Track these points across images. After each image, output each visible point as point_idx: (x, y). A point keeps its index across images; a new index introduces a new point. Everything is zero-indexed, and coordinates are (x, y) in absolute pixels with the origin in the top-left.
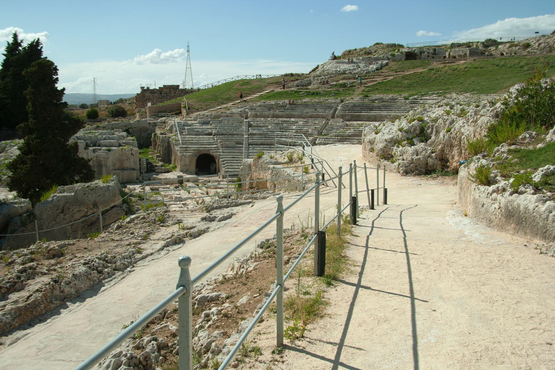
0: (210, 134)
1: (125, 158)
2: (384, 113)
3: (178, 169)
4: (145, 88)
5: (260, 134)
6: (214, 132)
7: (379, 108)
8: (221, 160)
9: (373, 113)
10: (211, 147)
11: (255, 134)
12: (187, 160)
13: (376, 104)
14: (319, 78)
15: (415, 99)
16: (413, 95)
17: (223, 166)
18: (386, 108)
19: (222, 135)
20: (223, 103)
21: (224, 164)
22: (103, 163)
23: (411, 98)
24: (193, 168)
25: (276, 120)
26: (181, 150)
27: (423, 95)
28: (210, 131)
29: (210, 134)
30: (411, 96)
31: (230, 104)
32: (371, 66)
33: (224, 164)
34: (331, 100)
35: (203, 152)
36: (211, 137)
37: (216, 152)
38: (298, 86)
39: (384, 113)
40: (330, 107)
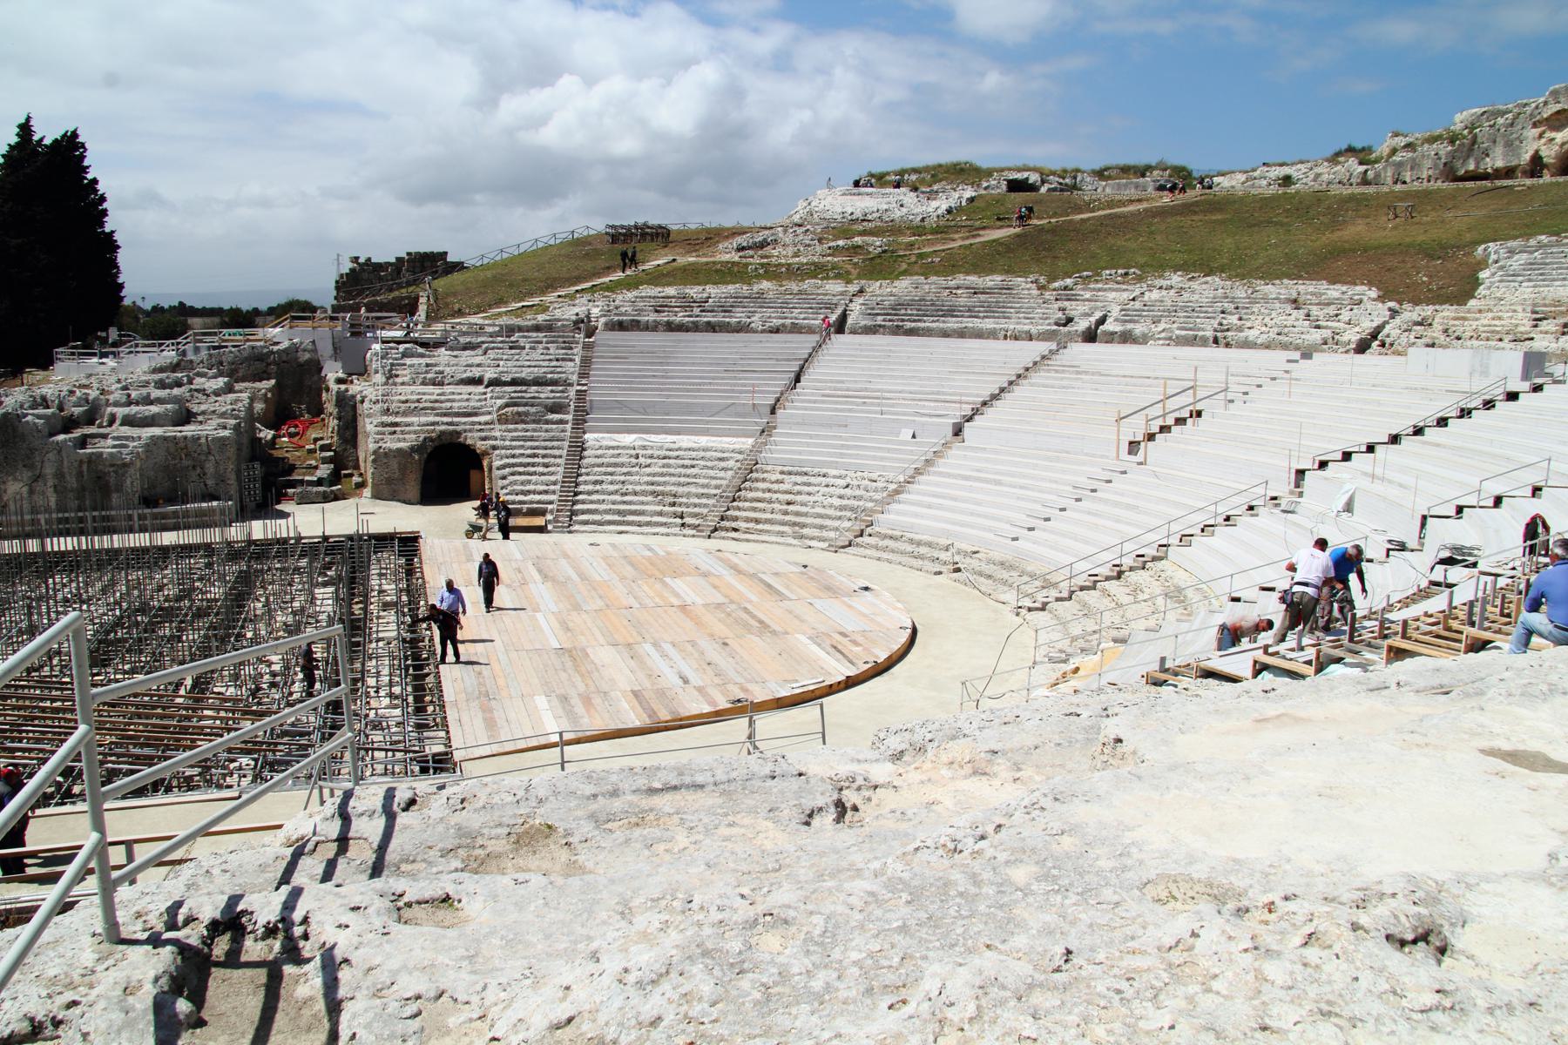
0: (477, 381)
1: (186, 463)
2: (988, 324)
3: (367, 492)
4: (362, 260)
6: (490, 374)
8: (497, 463)
9: (952, 324)
12: (394, 464)
13: (963, 300)
14: (800, 230)
15: (1066, 288)
17: (501, 483)
18: (990, 311)
19: (514, 382)
20: (531, 294)
21: (504, 478)
22: (112, 480)
24: (414, 489)
26: (378, 433)
28: (476, 373)
29: (477, 381)
31: (551, 297)
32: (934, 204)
33: (504, 478)
34: (835, 287)
36: (481, 389)
38: (743, 249)
39: (988, 324)
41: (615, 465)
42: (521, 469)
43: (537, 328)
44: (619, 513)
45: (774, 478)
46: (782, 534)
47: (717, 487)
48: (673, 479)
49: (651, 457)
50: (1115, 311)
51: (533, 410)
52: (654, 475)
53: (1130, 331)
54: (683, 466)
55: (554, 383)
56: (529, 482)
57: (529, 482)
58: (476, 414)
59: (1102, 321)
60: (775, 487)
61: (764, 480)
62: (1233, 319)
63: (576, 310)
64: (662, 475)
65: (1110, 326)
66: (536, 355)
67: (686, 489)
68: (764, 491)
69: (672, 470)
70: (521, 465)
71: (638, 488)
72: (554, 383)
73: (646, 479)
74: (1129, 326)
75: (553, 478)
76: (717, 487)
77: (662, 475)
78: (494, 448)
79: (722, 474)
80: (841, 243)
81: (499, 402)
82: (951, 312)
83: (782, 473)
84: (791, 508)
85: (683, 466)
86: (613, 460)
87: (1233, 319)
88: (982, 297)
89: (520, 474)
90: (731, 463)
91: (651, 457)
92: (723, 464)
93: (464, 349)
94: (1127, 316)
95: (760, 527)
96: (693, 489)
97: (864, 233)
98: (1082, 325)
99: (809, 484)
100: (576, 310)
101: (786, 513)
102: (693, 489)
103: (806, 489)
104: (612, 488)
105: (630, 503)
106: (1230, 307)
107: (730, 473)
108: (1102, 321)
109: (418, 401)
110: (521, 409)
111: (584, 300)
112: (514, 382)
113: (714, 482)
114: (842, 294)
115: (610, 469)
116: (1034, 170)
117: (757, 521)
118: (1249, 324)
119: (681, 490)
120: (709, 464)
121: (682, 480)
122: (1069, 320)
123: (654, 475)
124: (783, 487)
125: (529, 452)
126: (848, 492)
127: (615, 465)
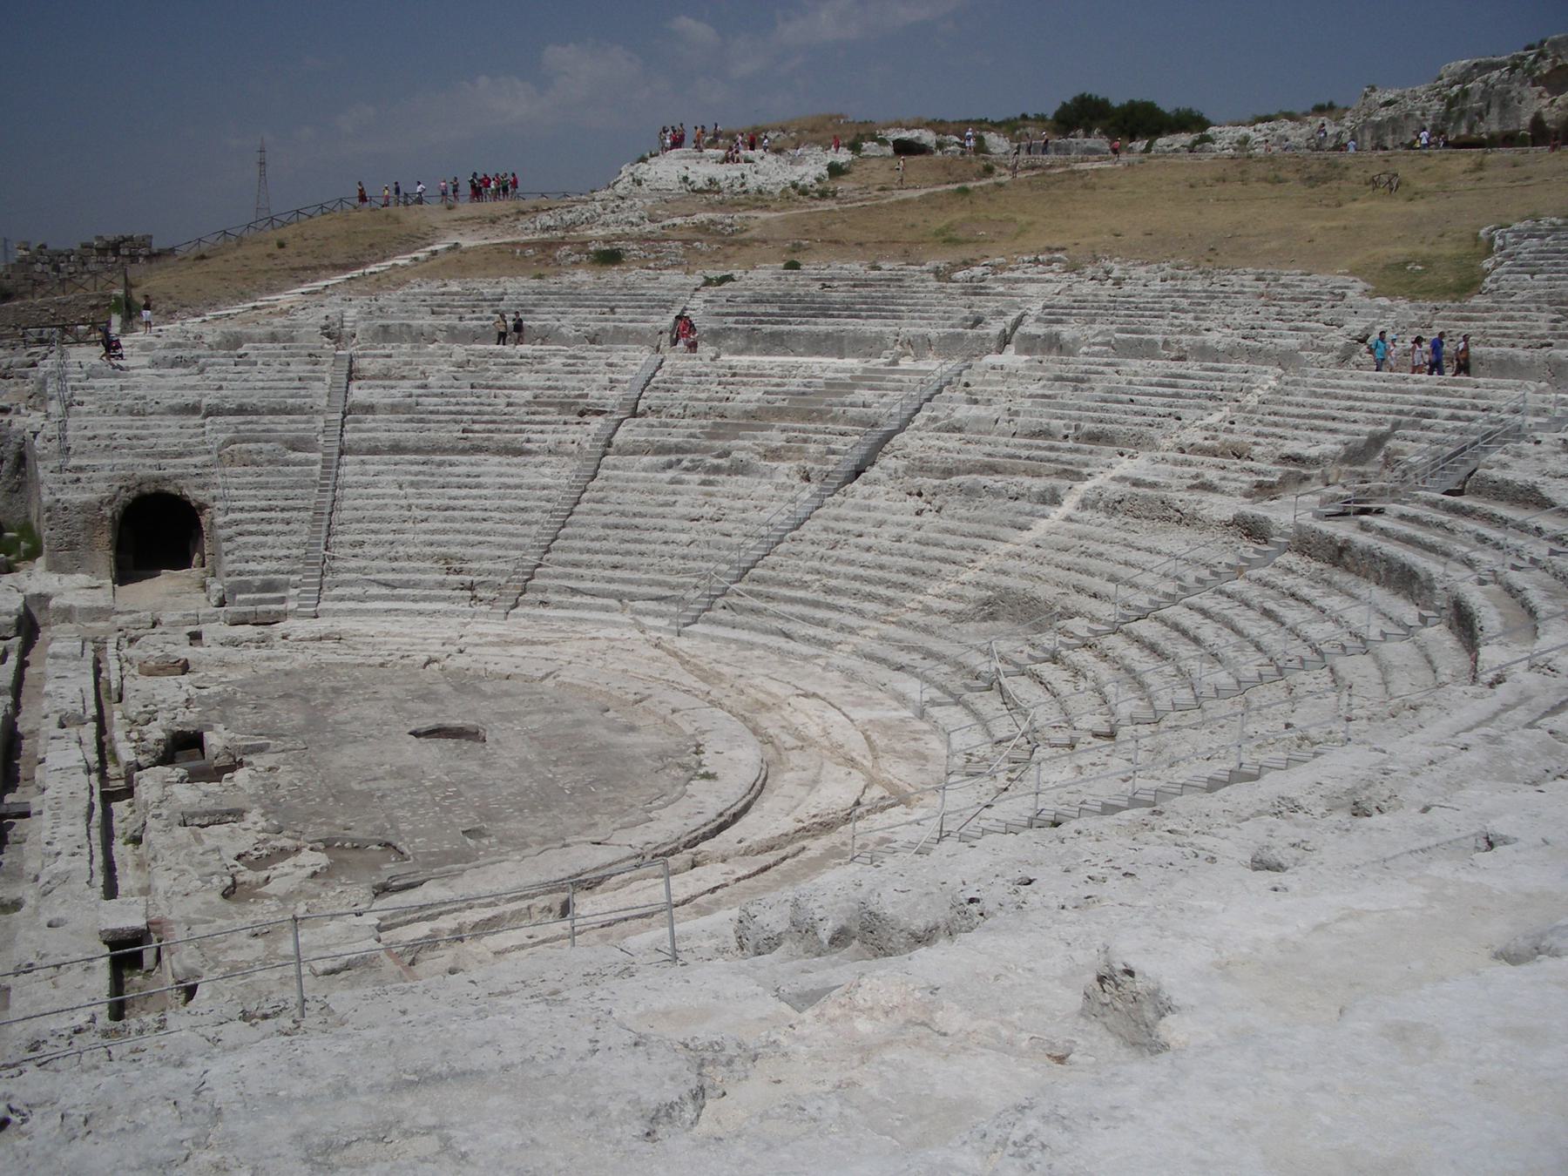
0: (193, 409)
5: (394, 409)
7: (850, 310)
10: (186, 466)
11: (370, 409)
16: (967, 264)
18: (875, 309)
19: (241, 410)
21: (229, 539)
23: (959, 275)
25: (459, 351)
27: (996, 268)
28: (190, 397)
29: (193, 409)
30: (955, 267)
33: (229, 539)
35: (146, 489)
36: (197, 420)
37: (203, 487)
39: (872, 327)
40: (665, 305)
41: (382, 520)
42: (253, 528)
43: (273, 338)
44: (386, 584)
45: (593, 533)
46: (607, 609)
47: (517, 547)
48: (460, 537)
49: (429, 508)
50: (1036, 308)
51: (269, 447)
52: (433, 532)
53: (1057, 335)
54: (472, 520)
55: (300, 410)
56: (263, 545)
57: (263, 545)
58: (191, 454)
59: (1019, 322)
60: (596, 545)
61: (582, 537)
62: (1188, 319)
63: (325, 311)
64: (445, 532)
65: (1031, 328)
66: (271, 372)
67: (477, 551)
68: (581, 551)
69: (457, 526)
70: (252, 521)
71: (412, 551)
72: (300, 410)
73: (423, 537)
74: (1057, 328)
75: (296, 539)
76: (517, 547)
77: (445, 532)
78: (215, 499)
79: (524, 529)
80: (678, 221)
81: (223, 437)
82: (824, 311)
83: (605, 526)
84: (618, 574)
85: (472, 520)
86: (377, 513)
87: (1188, 319)
88: (864, 291)
89: (251, 533)
90: (537, 515)
91: (429, 508)
92: (526, 516)
93: (174, 365)
94: (1053, 314)
95: (577, 599)
96: (485, 551)
97: (710, 207)
98: (995, 328)
99: (640, 541)
100: (325, 311)
101: (611, 581)
102: (485, 551)
103: (639, 547)
104: (376, 551)
105: (400, 571)
106: (1184, 303)
107: (535, 528)
108: (1019, 322)
109: (111, 437)
110: (252, 446)
111: (337, 299)
112: (241, 410)
113: (515, 540)
114: (682, 287)
115: (373, 526)
116: (929, 125)
117: (574, 591)
118: (1207, 324)
119: (469, 551)
120: (507, 516)
121: (471, 538)
122: (978, 321)
123: (433, 532)
124: (606, 545)
125: (264, 503)
126: (694, 550)
127: (382, 520)
